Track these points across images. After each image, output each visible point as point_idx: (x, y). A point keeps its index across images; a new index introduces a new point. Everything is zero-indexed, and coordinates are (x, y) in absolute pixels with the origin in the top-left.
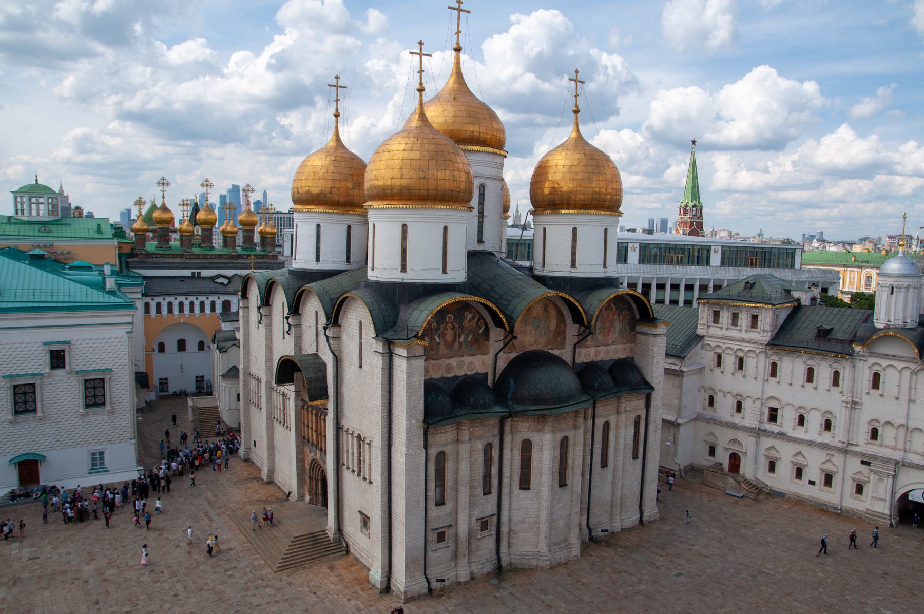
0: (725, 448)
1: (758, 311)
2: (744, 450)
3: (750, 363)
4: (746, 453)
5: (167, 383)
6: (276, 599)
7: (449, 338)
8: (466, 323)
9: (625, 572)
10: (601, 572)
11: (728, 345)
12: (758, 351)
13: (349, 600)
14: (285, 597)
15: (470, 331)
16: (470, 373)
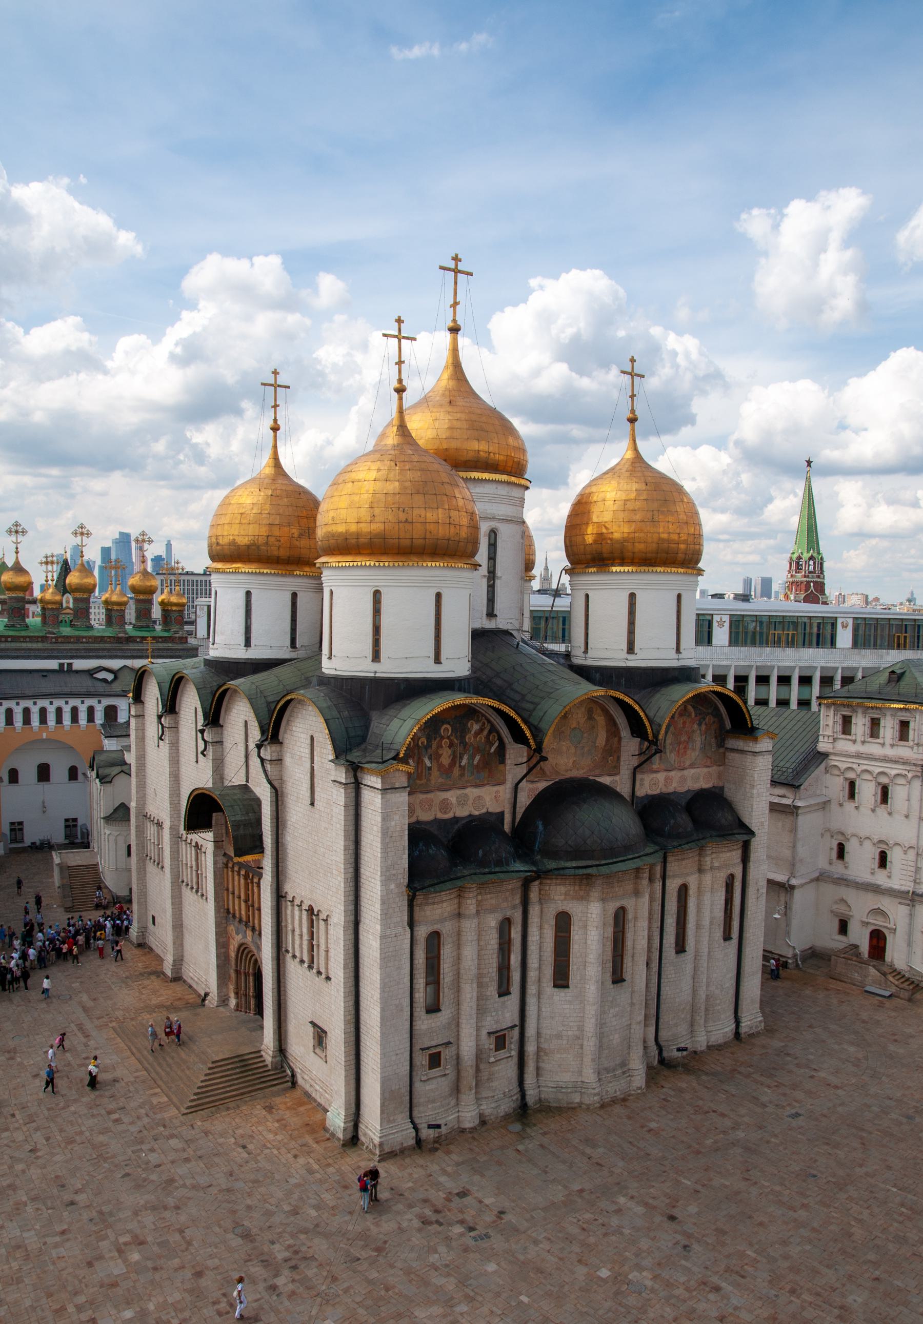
0: (863, 922)
1: (908, 714)
2: (891, 926)
3: (898, 794)
4: (895, 930)
5: (21, 830)
6: (185, 1155)
7: (446, 760)
8: (470, 738)
9: (714, 1111)
10: (678, 1112)
11: (865, 767)
12: (910, 775)
13: (295, 1156)
14: (199, 1153)
15: (477, 750)
16: (477, 813)
